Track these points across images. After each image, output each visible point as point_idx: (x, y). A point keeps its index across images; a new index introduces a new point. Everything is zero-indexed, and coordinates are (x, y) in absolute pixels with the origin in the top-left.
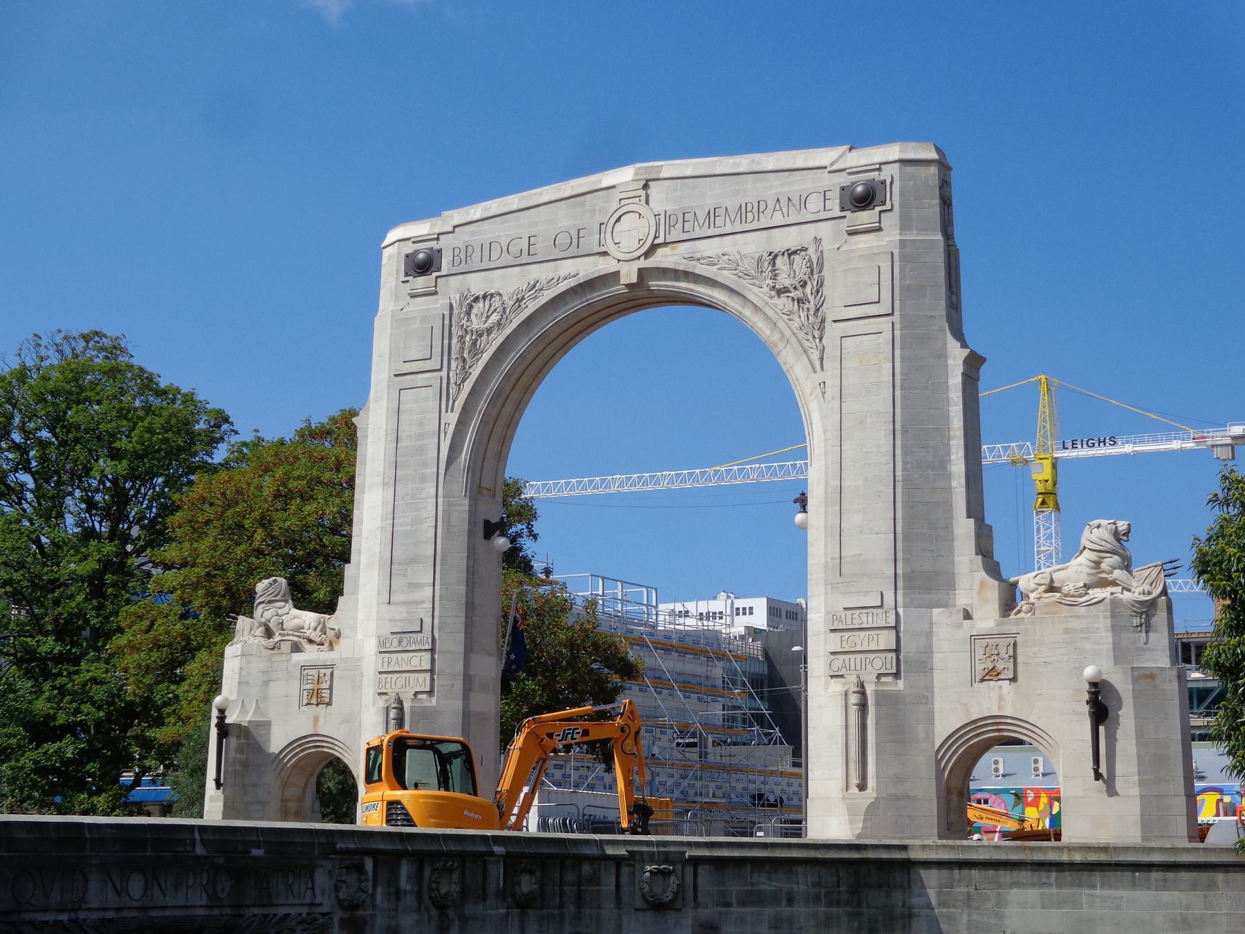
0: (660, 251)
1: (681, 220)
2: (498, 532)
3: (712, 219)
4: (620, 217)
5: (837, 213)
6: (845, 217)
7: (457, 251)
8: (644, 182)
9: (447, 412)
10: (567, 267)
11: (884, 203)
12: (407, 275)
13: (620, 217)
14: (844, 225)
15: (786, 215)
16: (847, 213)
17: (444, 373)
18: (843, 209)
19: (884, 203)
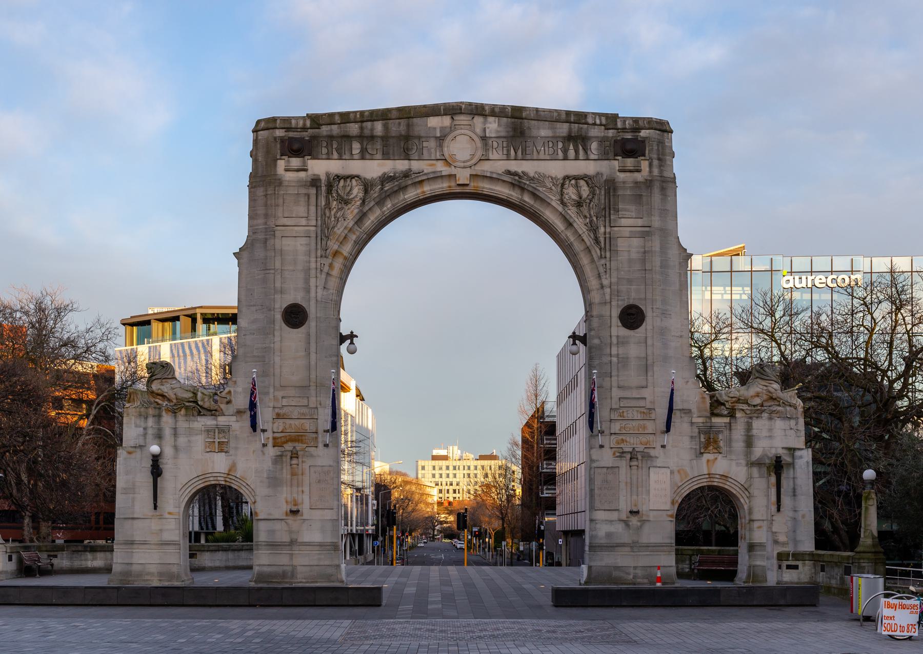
2: (349, 341)
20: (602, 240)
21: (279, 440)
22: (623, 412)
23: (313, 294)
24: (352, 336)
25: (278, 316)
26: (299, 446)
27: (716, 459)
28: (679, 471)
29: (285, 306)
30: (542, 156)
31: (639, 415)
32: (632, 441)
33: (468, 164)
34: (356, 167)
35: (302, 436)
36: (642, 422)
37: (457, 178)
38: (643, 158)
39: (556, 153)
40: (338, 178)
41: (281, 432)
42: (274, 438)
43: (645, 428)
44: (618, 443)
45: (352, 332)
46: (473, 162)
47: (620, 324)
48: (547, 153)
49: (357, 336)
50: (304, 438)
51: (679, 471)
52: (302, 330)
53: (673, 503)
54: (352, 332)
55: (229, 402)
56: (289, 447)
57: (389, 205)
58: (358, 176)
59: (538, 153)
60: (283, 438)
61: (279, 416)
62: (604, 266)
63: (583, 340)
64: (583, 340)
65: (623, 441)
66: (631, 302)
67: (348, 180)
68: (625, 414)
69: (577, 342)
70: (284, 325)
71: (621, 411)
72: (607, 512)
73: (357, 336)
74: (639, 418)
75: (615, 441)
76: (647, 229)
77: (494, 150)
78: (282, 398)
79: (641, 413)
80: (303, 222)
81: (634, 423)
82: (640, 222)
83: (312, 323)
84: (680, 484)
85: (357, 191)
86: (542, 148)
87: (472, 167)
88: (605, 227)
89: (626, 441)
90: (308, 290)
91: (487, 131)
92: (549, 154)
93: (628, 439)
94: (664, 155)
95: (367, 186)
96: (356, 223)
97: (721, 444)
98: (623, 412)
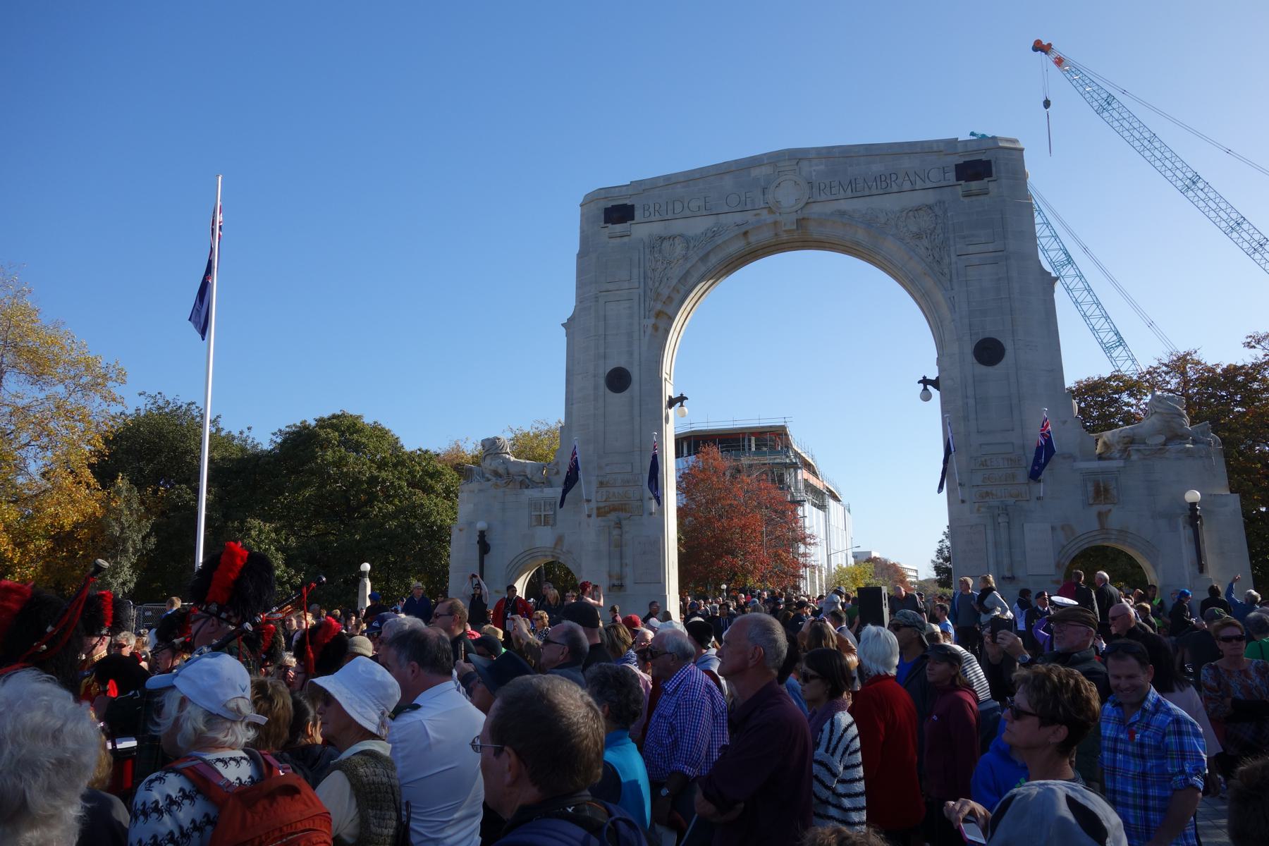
0: (814, 205)
1: (828, 186)
2: (679, 404)
3: (854, 186)
4: (779, 184)
5: (956, 183)
6: (961, 185)
7: (646, 208)
8: (796, 161)
9: (645, 318)
10: (738, 218)
11: (991, 176)
12: (605, 223)
13: (779, 184)
14: (959, 188)
15: (914, 183)
16: (962, 182)
17: (641, 291)
18: (958, 179)
19: (991, 176)
20: (946, 271)
21: (603, 510)
23: (636, 355)
24: (681, 399)
25: (602, 382)
26: (623, 515)
29: (608, 371)
30: (874, 191)
33: (795, 208)
34: (678, 227)
35: (625, 504)
37: (783, 224)
38: (990, 179)
39: (889, 185)
40: (662, 239)
41: (605, 501)
42: (598, 509)
44: (982, 497)
45: (682, 395)
46: (800, 206)
47: (975, 361)
48: (879, 187)
49: (686, 398)
50: (627, 506)
52: (626, 393)
53: (1058, 566)
54: (682, 395)
55: (557, 473)
56: (613, 516)
57: (713, 260)
58: (681, 236)
59: (870, 189)
60: (606, 508)
61: (601, 484)
62: (952, 299)
63: (935, 383)
64: (935, 383)
66: (987, 335)
67: (671, 240)
69: (929, 387)
70: (607, 390)
73: (686, 398)
76: (1001, 253)
77: (821, 192)
78: (607, 465)
80: (626, 285)
82: (991, 247)
83: (635, 385)
85: (679, 249)
86: (874, 184)
87: (799, 212)
88: (949, 256)
90: (631, 354)
91: (814, 174)
92: (881, 188)
94: (1018, 176)
95: (687, 240)
96: (679, 281)
97: (1114, 492)
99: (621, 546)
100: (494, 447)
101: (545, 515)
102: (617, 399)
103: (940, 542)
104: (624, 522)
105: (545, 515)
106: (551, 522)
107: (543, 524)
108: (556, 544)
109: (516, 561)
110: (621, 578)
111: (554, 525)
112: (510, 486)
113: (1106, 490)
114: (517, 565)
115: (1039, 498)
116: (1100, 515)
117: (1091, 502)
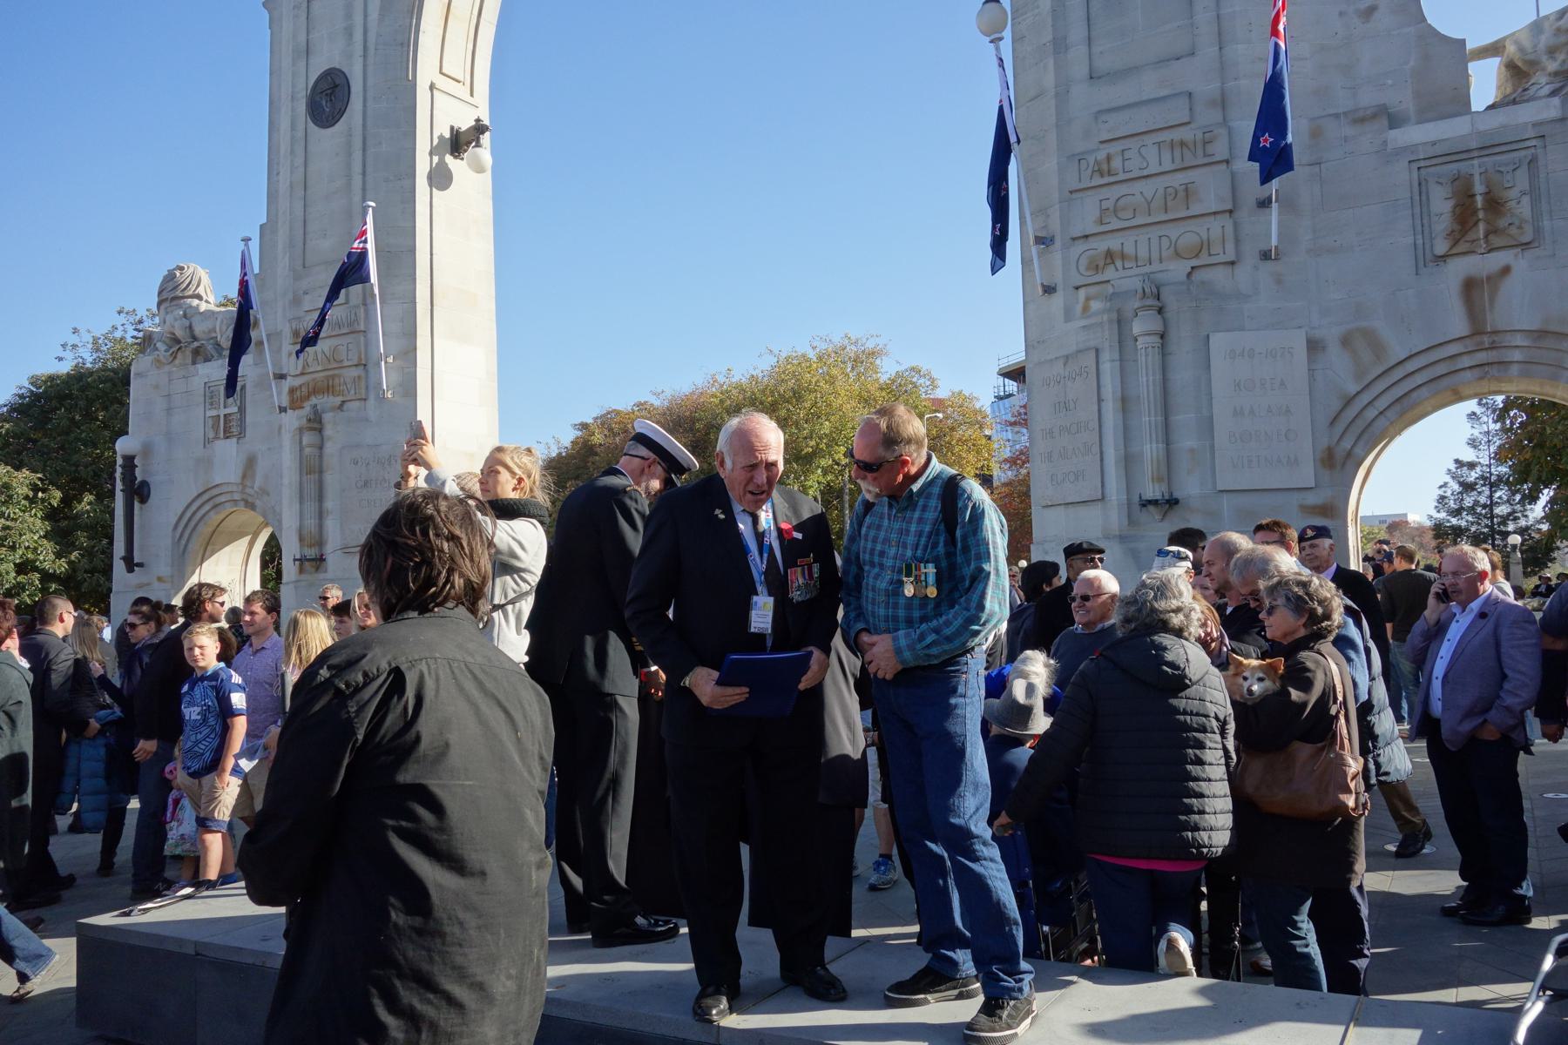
22: (1109, 158)
27: (1506, 270)
28: (1346, 341)
31: (1166, 156)
32: (1143, 253)
35: (333, 377)
36: (1178, 180)
41: (302, 374)
43: (1188, 193)
50: (337, 381)
51: (1346, 341)
65: (1110, 256)
68: (1117, 163)
70: (311, 124)
71: (1101, 155)
72: (1071, 509)
74: (1167, 166)
75: (1083, 262)
79: (1172, 145)
81: (1147, 188)
84: (1353, 388)
89: (1123, 257)
93: (1129, 249)
98: (1109, 158)
99: (321, 472)
100: (171, 285)
101: (225, 415)
102: (327, 140)
103: (1441, 487)
104: (327, 417)
105: (225, 415)
106: (235, 430)
107: (222, 435)
108: (244, 476)
109: (188, 514)
110: (320, 542)
111: (241, 435)
112: (177, 362)
113: (1495, 204)
114: (192, 524)
115: (1266, 256)
116: (1470, 287)
117: (1441, 247)
